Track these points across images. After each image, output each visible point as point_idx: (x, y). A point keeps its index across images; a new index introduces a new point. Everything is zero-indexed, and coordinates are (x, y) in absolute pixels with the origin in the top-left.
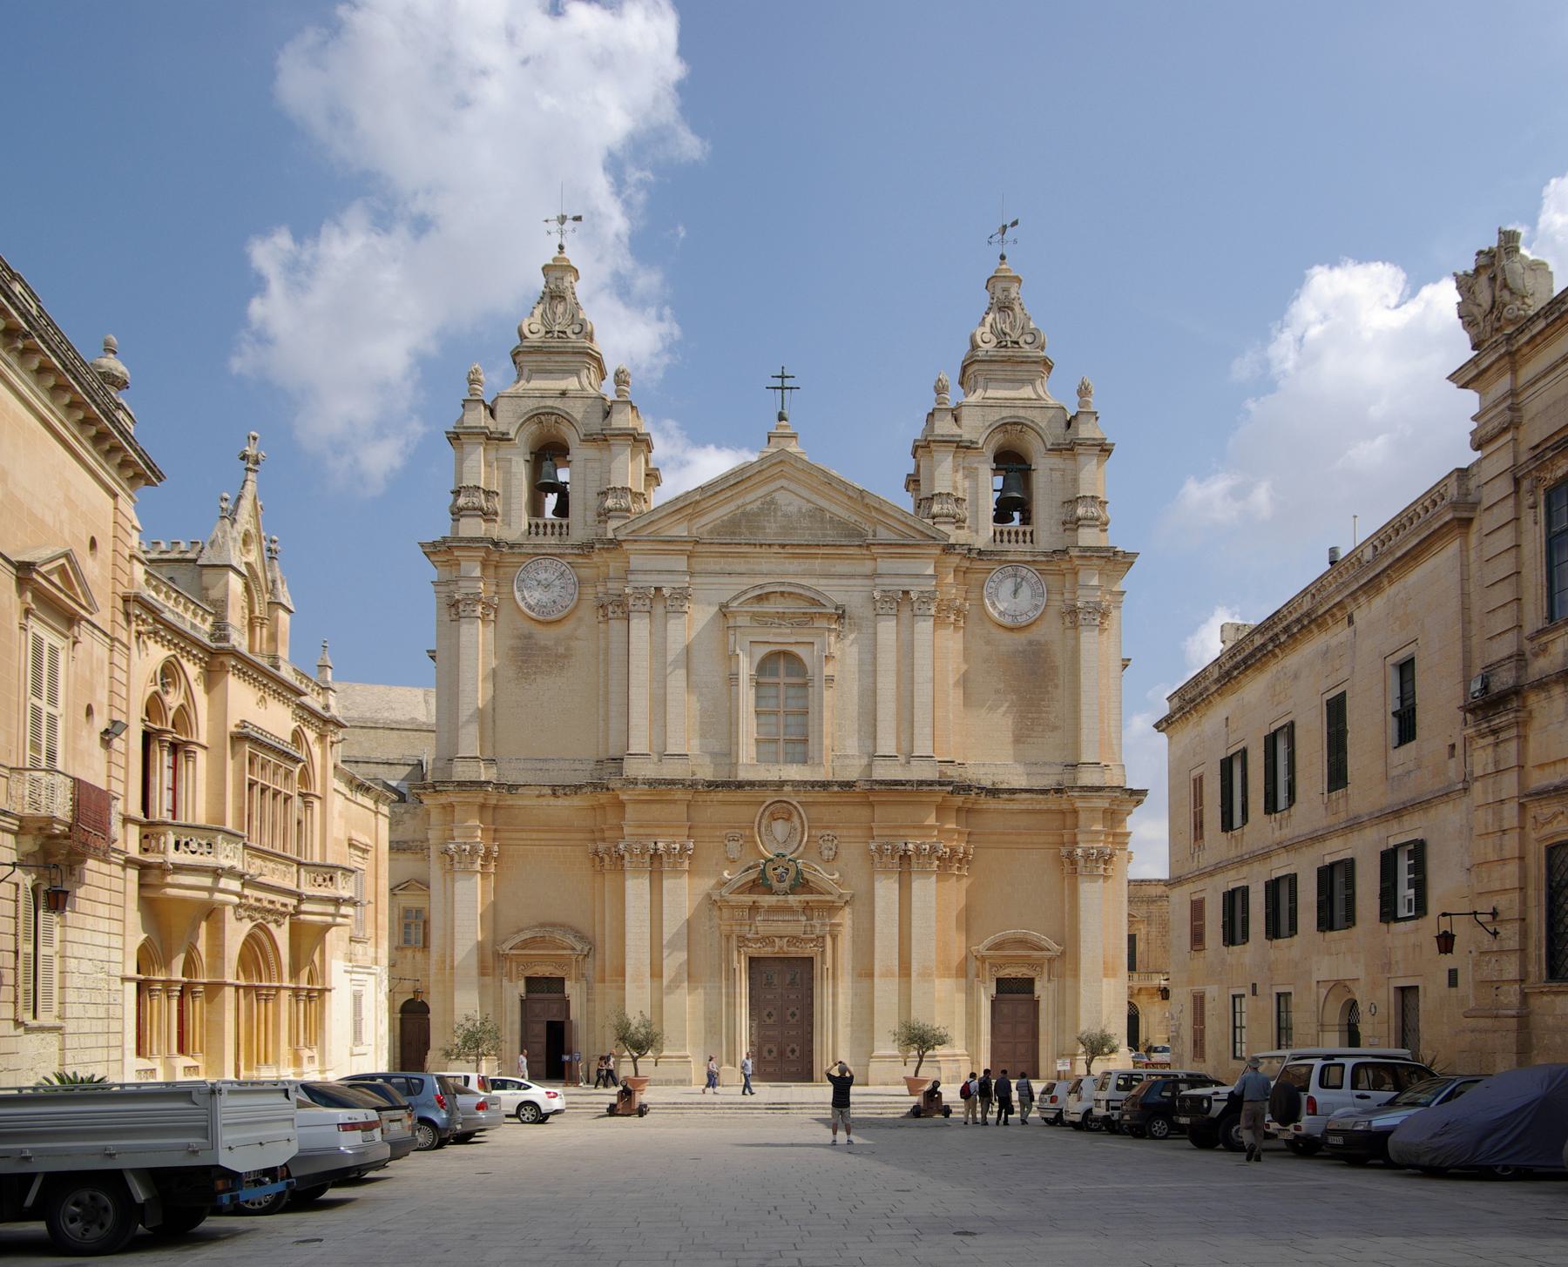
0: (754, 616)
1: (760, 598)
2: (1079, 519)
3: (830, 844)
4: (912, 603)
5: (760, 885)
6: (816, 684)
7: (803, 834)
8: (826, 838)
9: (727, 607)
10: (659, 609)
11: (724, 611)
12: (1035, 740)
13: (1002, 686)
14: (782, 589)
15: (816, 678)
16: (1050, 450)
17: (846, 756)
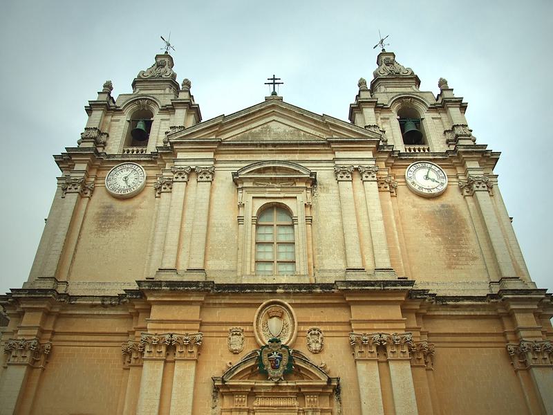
0: (255, 180)
1: (259, 171)
2: (457, 136)
3: (316, 337)
4: (361, 175)
5: (259, 370)
6: (299, 222)
7: (293, 329)
8: (313, 332)
9: (237, 175)
10: (193, 181)
11: (237, 180)
12: (463, 267)
13: (429, 232)
14: (274, 165)
15: (299, 219)
16: (429, 108)
17: (324, 271)
